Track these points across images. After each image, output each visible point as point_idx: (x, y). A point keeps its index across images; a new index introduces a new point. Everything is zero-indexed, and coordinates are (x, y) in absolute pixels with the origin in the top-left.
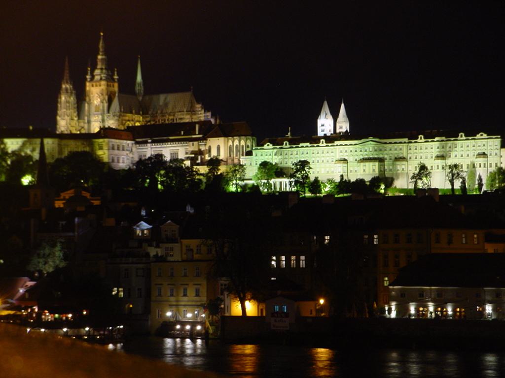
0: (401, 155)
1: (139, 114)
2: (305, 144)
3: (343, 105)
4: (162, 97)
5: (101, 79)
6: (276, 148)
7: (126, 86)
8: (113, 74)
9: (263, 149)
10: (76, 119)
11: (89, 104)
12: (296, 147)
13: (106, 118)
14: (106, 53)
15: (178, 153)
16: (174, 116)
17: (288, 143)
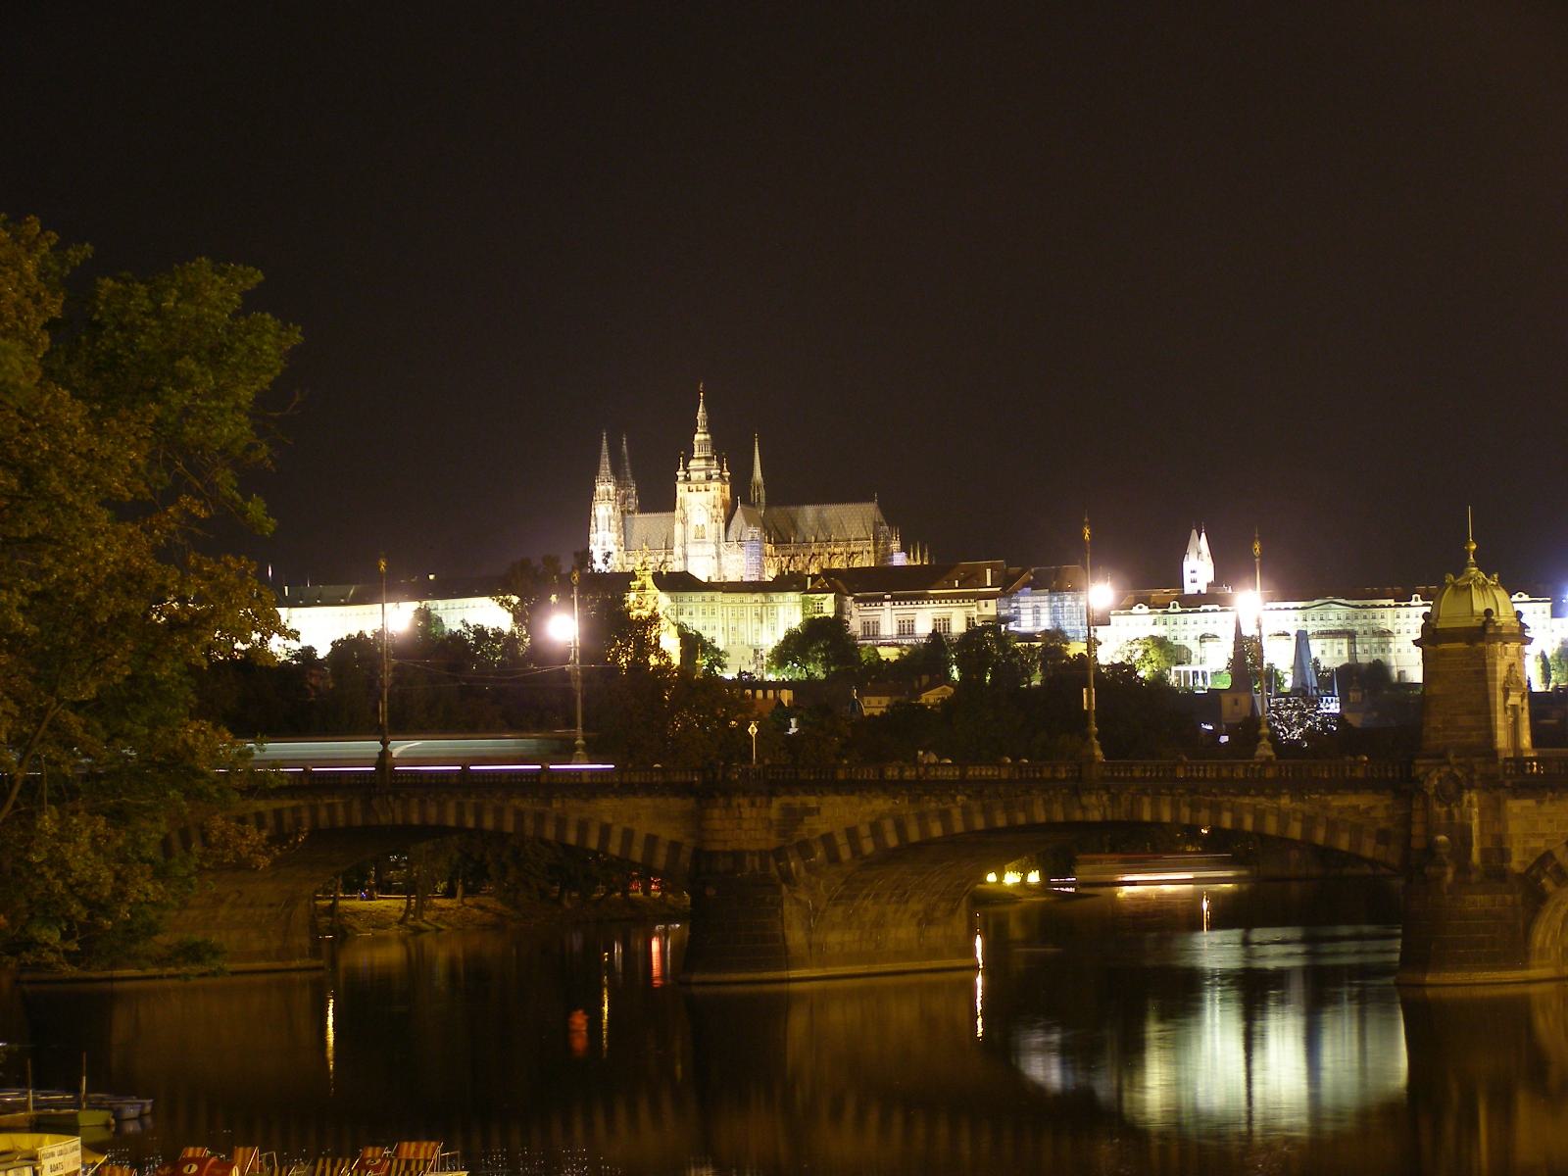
0: (1383, 627)
1: (770, 543)
2: (1210, 607)
3: (1203, 535)
4: (810, 512)
5: (709, 478)
6: (1157, 613)
7: (740, 493)
8: (722, 470)
9: (1131, 614)
10: (623, 549)
11: (684, 522)
12: (1192, 612)
13: (722, 550)
14: (710, 430)
15: (948, 620)
16: (849, 545)
17: (1177, 603)
